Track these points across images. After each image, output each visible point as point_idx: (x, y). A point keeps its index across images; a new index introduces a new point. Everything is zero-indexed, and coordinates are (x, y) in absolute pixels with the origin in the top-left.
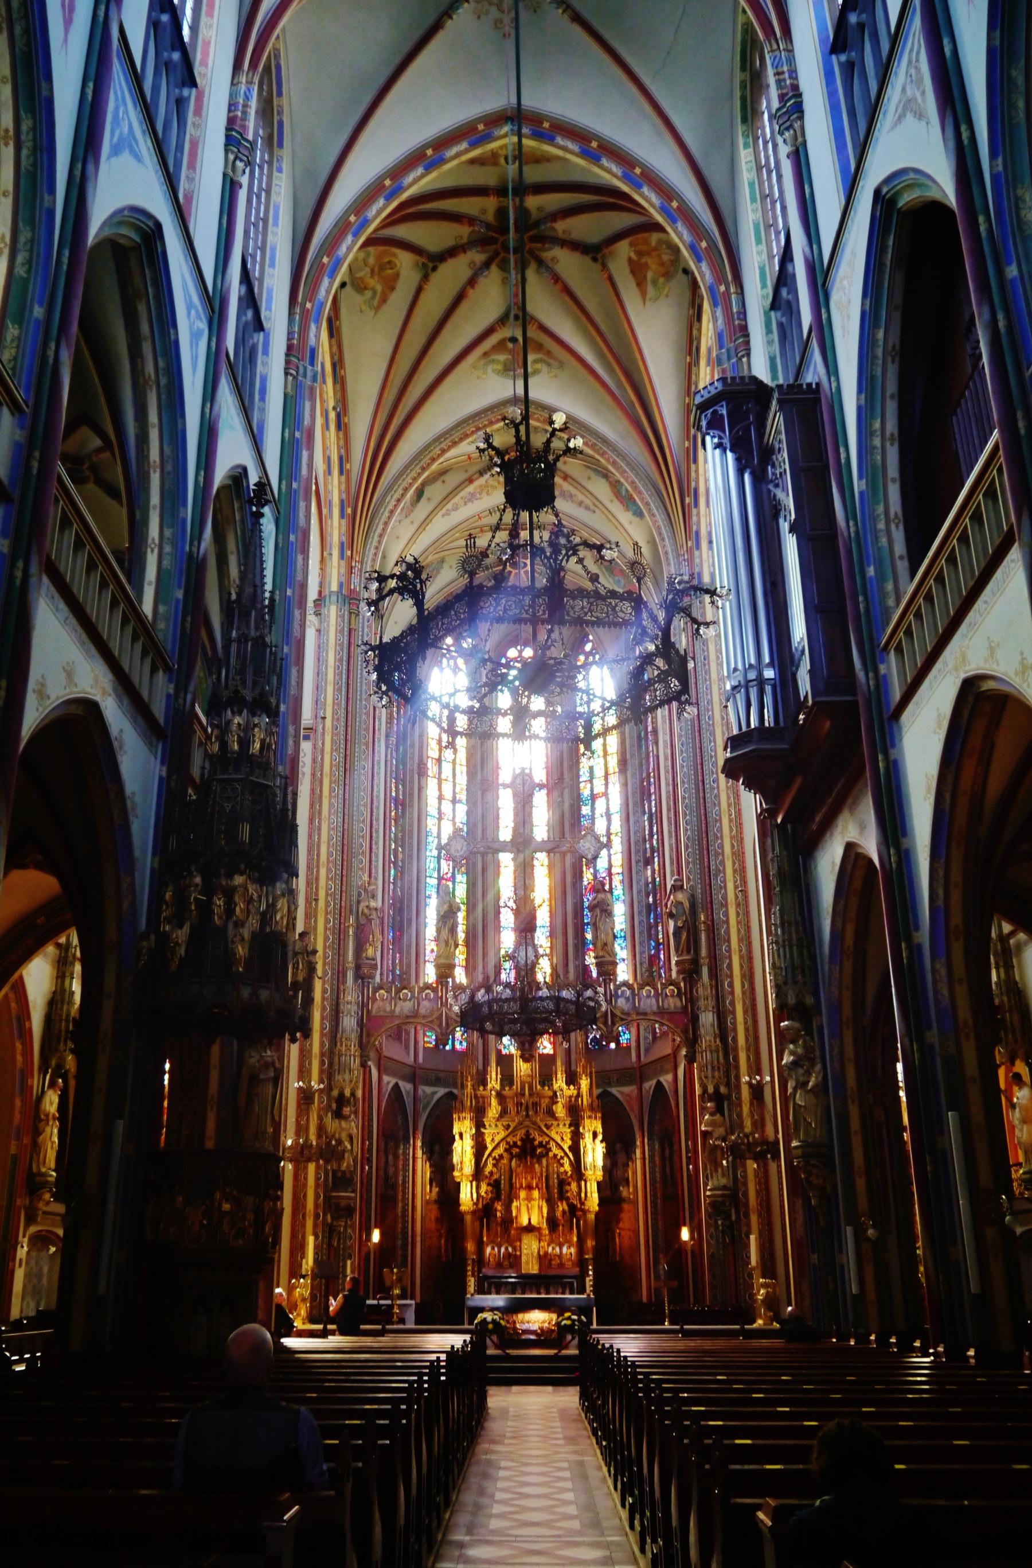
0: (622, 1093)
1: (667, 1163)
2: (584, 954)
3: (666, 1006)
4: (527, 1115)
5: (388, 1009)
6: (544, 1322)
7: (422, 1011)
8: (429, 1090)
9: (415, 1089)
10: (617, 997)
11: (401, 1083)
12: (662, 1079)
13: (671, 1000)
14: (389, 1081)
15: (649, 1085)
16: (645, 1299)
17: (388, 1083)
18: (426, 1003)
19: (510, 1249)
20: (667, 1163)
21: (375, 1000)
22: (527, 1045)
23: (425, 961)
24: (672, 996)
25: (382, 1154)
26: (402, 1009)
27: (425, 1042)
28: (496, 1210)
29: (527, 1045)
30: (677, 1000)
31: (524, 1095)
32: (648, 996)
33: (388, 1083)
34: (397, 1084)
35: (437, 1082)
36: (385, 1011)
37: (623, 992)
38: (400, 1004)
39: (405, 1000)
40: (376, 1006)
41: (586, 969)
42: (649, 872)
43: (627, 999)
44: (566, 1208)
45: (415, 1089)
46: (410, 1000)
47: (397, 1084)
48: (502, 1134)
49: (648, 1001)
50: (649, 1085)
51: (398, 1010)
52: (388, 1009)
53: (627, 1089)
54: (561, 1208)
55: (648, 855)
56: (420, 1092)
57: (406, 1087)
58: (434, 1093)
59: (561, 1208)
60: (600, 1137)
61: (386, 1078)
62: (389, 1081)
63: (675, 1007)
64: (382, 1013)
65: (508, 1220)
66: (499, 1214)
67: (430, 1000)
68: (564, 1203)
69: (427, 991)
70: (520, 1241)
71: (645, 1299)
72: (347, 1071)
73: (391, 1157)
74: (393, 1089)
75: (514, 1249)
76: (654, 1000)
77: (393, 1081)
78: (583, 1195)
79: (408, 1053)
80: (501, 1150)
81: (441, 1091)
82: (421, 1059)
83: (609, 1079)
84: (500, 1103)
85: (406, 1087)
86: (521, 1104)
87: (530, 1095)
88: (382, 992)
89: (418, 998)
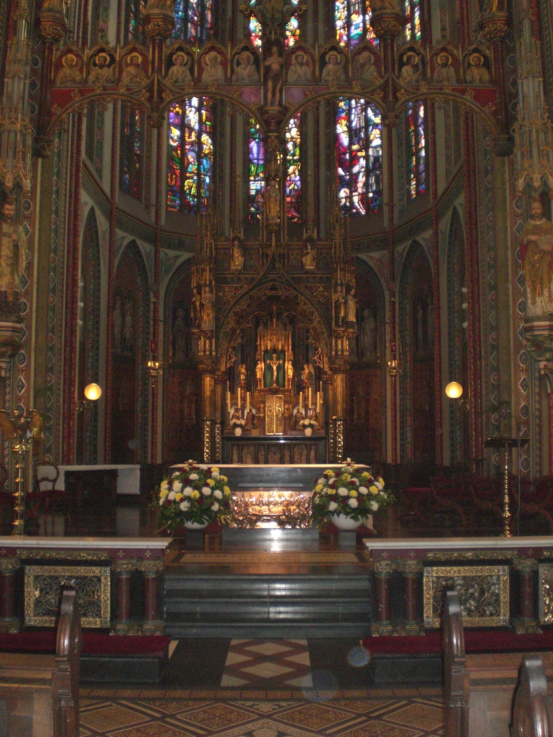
0: (372, 258)
1: (420, 326)
2: (335, 123)
3: (469, 78)
4: (274, 268)
5: (78, 78)
6: (289, 504)
7: (126, 80)
8: (172, 253)
9: (157, 252)
10: (402, 64)
11: (138, 242)
12: (419, 239)
13: (475, 71)
14: (125, 238)
15: (402, 248)
16: (389, 461)
17: (123, 238)
18: (132, 70)
19: (254, 411)
20: (420, 326)
21: (59, 66)
22: (273, 124)
23: (169, 124)
24: (477, 66)
25: (117, 314)
26: (97, 78)
27: (168, 206)
28: (240, 373)
29: (273, 124)
30: (484, 71)
31: (271, 245)
32: (444, 65)
33: (123, 238)
34: (133, 242)
35: (181, 246)
36: (73, 81)
37: (409, 58)
38: (96, 70)
39: (101, 67)
40: (61, 74)
41: (336, 137)
42: (408, 33)
43: (415, 67)
44: (312, 371)
45: (157, 252)
46: (109, 66)
47: (133, 242)
48: (246, 287)
49: (444, 70)
50: (402, 248)
51: (91, 78)
52: (78, 78)
53: (376, 255)
54: (307, 371)
55: (408, 12)
56: (162, 254)
57: (145, 247)
58: (177, 257)
59: (307, 371)
60: (353, 292)
61: (119, 233)
62: (125, 238)
63: (481, 81)
64: (69, 84)
65: (251, 383)
66: (242, 377)
67: (137, 66)
68: (310, 366)
69: (134, 54)
70: (264, 403)
71: (389, 461)
72: (11, 152)
73: (128, 318)
74: (128, 247)
75: (258, 410)
76: (452, 70)
77: (130, 238)
78: (333, 353)
79: (149, 213)
80: (243, 305)
81: (185, 256)
82: (163, 222)
83: (359, 245)
84: (244, 256)
85: (145, 247)
86: (267, 255)
87: (277, 246)
88: (70, 56)
89: (120, 64)
